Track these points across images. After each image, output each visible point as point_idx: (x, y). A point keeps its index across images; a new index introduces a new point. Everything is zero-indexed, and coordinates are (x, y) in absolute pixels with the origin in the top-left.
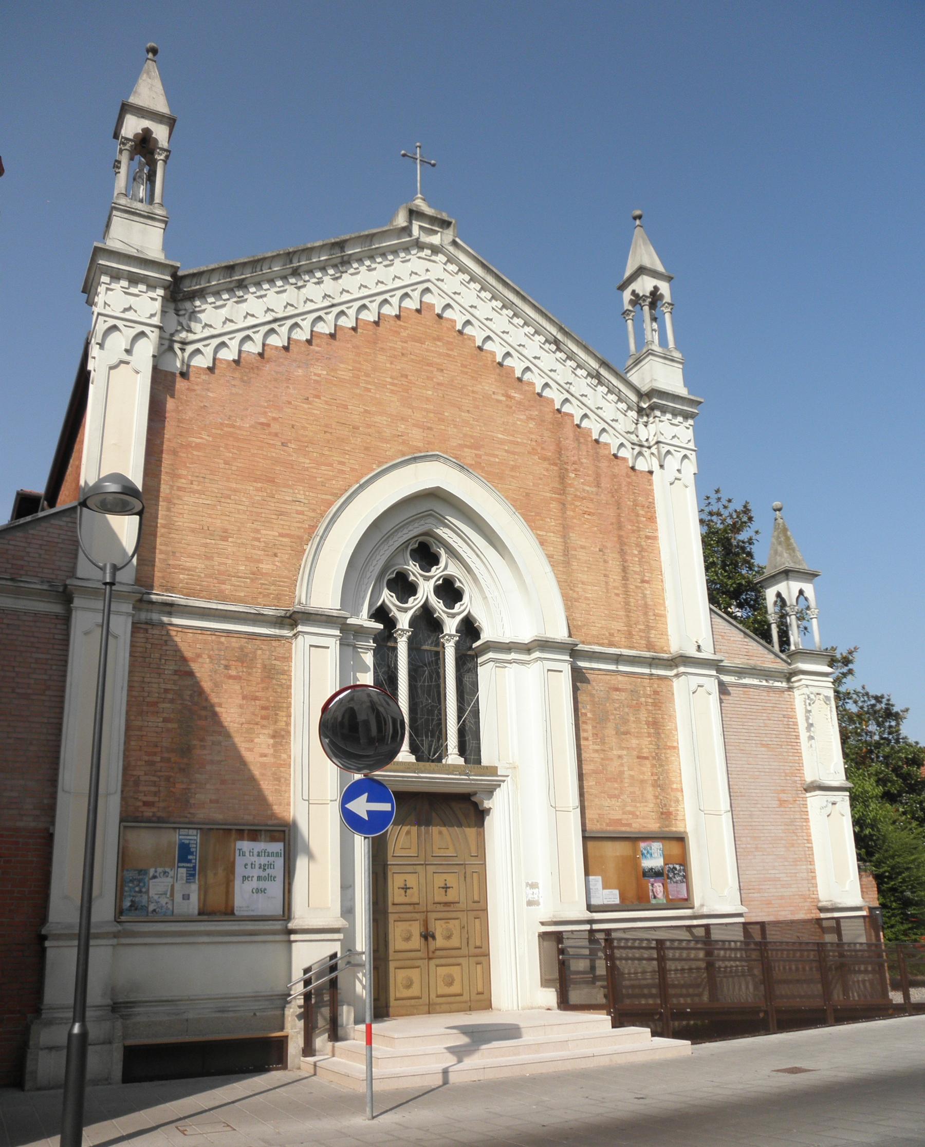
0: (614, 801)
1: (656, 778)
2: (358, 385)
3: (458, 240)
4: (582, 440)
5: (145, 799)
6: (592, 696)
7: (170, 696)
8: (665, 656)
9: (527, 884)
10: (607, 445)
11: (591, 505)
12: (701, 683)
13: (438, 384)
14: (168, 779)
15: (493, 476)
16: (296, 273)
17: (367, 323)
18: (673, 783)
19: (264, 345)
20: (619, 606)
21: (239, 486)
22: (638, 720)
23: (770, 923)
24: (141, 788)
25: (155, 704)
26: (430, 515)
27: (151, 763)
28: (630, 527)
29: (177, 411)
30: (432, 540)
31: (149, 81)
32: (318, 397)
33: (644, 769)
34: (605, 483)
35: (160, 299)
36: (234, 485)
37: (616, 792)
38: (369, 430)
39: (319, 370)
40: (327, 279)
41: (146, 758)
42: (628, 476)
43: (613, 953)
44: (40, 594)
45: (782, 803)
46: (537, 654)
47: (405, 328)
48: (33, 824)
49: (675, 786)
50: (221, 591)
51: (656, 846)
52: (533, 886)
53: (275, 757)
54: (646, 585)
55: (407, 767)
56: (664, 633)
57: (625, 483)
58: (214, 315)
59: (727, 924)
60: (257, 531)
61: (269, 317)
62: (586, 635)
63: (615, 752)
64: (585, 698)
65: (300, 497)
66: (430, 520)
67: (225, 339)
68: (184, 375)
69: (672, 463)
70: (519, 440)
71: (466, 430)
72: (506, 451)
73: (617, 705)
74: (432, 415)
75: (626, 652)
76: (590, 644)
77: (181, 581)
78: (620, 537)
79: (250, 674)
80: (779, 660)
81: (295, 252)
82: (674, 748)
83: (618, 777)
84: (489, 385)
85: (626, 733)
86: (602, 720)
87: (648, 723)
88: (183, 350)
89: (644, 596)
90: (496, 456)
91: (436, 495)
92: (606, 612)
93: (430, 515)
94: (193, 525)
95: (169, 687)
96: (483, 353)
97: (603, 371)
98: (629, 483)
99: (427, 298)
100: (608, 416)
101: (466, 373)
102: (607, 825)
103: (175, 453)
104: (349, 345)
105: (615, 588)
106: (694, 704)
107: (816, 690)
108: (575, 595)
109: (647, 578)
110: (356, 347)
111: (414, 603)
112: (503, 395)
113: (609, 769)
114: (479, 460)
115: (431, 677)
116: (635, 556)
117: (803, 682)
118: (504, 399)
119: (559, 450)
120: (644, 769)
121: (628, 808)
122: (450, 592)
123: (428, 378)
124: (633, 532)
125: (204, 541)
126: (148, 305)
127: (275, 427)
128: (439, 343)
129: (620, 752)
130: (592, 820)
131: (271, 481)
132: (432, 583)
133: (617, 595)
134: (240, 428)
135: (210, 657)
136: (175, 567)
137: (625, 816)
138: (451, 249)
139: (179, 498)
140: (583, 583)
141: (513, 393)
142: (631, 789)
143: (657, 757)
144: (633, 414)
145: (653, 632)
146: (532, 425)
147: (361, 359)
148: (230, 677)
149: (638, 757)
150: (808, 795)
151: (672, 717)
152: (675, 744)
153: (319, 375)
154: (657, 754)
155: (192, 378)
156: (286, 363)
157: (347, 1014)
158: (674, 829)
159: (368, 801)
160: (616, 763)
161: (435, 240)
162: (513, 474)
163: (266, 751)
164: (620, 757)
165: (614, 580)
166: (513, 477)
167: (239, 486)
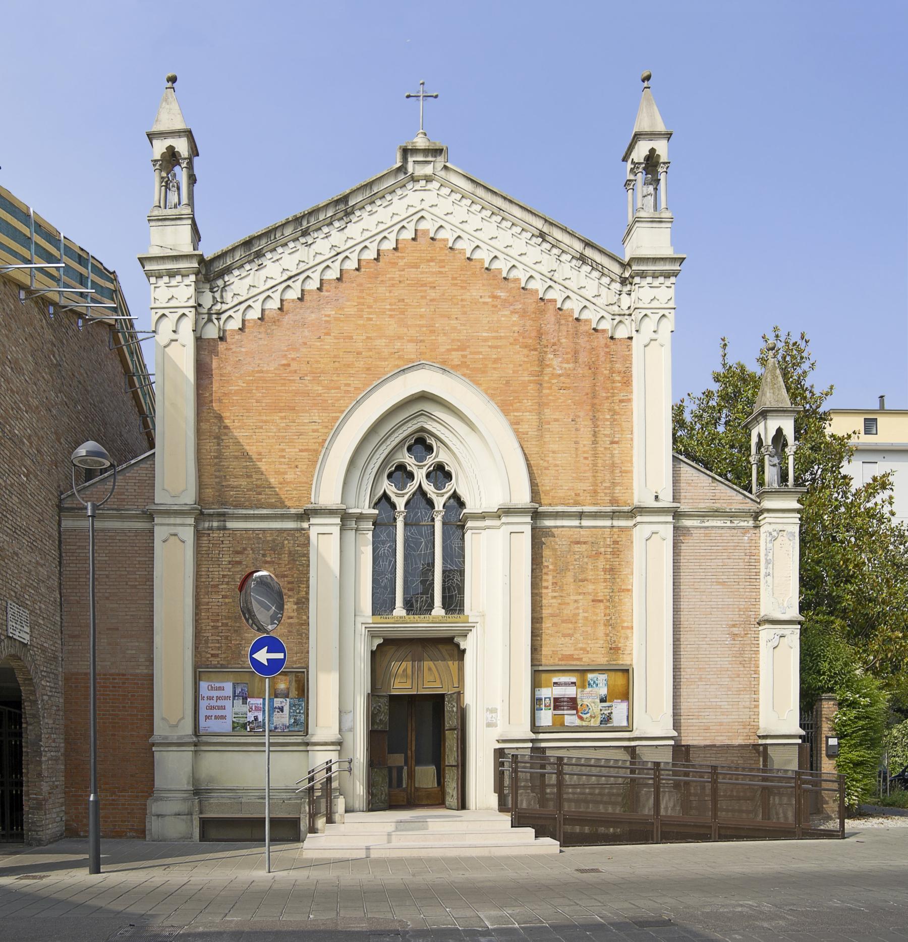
0: (567, 639)
1: (608, 618)
2: (361, 317)
3: (448, 164)
4: (563, 322)
5: (212, 652)
6: (554, 550)
7: (226, 580)
8: (626, 509)
9: (488, 709)
10: (588, 321)
11: (568, 381)
12: (655, 530)
13: (431, 300)
14: (226, 638)
15: (472, 372)
16: (305, 233)
17: (368, 262)
18: (624, 621)
19: (282, 301)
20: (587, 468)
21: (268, 418)
22: (595, 568)
23: (694, 746)
24: (210, 645)
25: (216, 586)
26: (422, 414)
27: (217, 627)
28: (604, 395)
29: (220, 368)
30: (426, 435)
31: (167, 106)
32: (328, 334)
33: (598, 611)
34: (583, 357)
35: (193, 284)
36: (264, 418)
37: (570, 632)
38: (371, 353)
39: (329, 311)
40: (334, 232)
41: (212, 624)
42: (607, 346)
43: (517, 767)
44: (136, 517)
45: (734, 636)
46: (504, 519)
47: (403, 258)
48: (146, 671)
49: (625, 624)
50: (259, 500)
51: (602, 678)
52: (493, 711)
53: (298, 618)
54: (615, 446)
55: (401, 620)
56: (629, 488)
57: (602, 354)
58: (240, 284)
59: (657, 746)
60: (283, 450)
61: (285, 277)
62: (553, 497)
63: (572, 597)
64: (548, 553)
65: (316, 418)
66: (422, 419)
67: (250, 302)
68: (221, 339)
69: (649, 325)
70: (502, 335)
71: (454, 336)
72: (489, 347)
73: (577, 557)
74: (425, 329)
75: (587, 509)
76: (556, 505)
77: (231, 496)
78: (593, 405)
79: (280, 559)
80: (749, 501)
81: (303, 216)
82: (628, 590)
83: (573, 620)
84: (478, 291)
85: (582, 581)
86: (561, 571)
87: (605, 570)
88: (218, 319)
89: (613, 456)
90: (480, 353)
91: (423, 397)
92: (574, 475)
93: (422, 414)
94: (236, 454)
95: (225, 573)
96: (472, 263)
97: (589, 252)
98: (608, 353)
99: (423, 226)
100: (589, 293)
101: (456, 285)
102: (560, 660)
103: (220, 401)
104: (354, 285)
105: (584, 452)
106: (650, 551)
107: (780, 527)
108: (545, 464)
109: (616, 439)
110: (361, 285)
111: (412, 487)
112: (489, 297)
113: (565, 612)
114: (464, 360)
115: (427, 546)
116: (607, 420)
117: (767, 520)
118: (490, 300)
119: (540, 336)
120: (598, 611)
121: (580, 645)
122: (441, 474)
123: (422, 297)
124: (607, 398)
125: (245, 464)
126: (184, 291)
127: (294, 366)
128: (432, 264)
129: (576, 597)
130: (546, 656)
131: (293, 409)
132: (424, 471)
133: (586, 458)
134: (267, 372)
135: (252, 549)
136: (227, 486)
137: (577, 652)
138: (443, 174)
139: (226, 434)
140: (554, 452)
141: (499, 293)
142: (584, 629)
143: (611, 600)
144: (616, 286)
145: (618, 488)
146: (515, 318)
147: (364, 295)
148: (267, 562)
149: (593, 601)
150: (761, 628)
151: (630, 564)
152: (630, 587)
153: (329, 316)
154: (611, 597)
155: (228, 340)
156: (301, 311)
157: (340, 804)
158: (621, 662)
159: (268, 652)
160: (572, 606)
161: (428, 170)
162: (494, 366)
163: (292, 614)
164: (576, 601)
165: (584, 446)
166: (494, 369)
167: (268, 418)
